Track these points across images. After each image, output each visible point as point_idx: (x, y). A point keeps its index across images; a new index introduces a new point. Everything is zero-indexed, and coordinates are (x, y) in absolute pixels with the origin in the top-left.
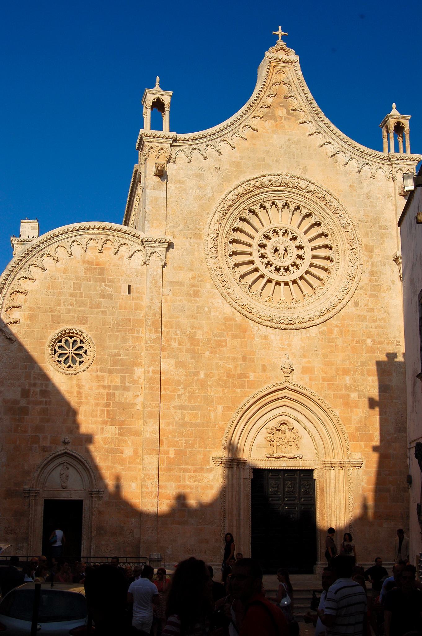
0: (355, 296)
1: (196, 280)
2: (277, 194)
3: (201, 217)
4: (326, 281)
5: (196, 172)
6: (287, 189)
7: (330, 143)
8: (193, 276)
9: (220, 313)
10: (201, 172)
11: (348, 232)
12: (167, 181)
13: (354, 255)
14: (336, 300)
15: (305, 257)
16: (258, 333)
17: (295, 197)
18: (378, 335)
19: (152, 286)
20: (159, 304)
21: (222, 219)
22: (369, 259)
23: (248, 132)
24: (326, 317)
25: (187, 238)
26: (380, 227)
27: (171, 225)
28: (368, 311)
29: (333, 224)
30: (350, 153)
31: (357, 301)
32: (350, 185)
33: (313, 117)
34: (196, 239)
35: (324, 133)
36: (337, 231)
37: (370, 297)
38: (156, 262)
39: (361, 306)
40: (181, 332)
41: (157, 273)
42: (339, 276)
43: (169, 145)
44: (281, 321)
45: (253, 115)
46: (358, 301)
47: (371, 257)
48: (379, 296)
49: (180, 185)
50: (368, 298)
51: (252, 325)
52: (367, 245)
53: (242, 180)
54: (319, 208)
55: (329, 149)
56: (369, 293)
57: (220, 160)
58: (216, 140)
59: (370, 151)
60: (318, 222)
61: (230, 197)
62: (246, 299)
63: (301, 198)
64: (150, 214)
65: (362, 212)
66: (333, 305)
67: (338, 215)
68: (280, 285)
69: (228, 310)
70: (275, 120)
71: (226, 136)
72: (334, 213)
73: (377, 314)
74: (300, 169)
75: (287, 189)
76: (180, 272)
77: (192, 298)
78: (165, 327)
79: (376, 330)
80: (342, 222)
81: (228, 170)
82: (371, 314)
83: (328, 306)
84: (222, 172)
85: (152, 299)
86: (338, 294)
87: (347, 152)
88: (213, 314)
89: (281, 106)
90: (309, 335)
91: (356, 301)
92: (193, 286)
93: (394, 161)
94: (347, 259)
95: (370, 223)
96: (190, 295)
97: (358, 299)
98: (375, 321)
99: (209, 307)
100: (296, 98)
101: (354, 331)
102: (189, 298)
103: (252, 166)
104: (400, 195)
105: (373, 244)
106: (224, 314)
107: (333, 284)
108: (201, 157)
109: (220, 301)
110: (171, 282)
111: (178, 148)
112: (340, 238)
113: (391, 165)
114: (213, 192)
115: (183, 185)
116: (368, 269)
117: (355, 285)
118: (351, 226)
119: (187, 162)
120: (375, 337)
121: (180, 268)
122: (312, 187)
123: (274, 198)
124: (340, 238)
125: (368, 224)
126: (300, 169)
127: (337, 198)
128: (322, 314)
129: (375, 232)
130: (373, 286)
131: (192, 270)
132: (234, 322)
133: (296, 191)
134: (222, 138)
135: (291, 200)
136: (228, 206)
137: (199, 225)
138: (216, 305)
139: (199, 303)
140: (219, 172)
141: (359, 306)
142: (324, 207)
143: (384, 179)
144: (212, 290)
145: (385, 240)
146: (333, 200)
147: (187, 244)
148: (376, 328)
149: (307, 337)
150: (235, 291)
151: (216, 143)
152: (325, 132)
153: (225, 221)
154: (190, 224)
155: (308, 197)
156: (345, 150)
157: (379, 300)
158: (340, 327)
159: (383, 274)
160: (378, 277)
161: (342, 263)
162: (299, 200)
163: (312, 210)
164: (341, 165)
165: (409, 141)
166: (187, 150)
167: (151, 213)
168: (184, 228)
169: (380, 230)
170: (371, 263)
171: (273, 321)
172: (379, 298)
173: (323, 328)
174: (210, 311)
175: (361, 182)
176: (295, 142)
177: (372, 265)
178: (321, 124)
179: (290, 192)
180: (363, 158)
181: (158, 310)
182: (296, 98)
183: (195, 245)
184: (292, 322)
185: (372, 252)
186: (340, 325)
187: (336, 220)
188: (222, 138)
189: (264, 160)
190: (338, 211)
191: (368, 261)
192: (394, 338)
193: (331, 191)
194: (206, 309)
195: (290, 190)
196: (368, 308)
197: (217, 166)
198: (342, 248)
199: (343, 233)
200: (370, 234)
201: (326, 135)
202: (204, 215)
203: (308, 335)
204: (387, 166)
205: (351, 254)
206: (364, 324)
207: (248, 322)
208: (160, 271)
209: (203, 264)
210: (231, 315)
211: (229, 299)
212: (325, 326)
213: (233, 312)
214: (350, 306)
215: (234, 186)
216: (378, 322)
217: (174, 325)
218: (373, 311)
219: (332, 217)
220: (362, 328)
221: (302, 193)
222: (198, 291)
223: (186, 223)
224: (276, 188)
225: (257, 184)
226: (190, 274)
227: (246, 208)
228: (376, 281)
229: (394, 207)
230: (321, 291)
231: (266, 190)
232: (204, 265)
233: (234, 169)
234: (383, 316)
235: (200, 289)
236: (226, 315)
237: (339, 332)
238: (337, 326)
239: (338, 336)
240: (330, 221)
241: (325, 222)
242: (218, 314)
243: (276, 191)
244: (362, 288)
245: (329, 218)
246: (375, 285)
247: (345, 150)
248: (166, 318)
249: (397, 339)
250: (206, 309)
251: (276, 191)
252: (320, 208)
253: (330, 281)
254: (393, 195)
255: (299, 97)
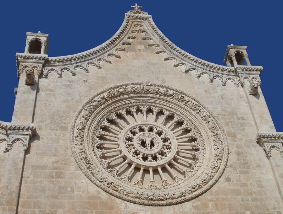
0: (225, 173)
1: (60, 163)
2: (141, 100)
3: (68, 115)
4: (194, 166)
5: (66, 84)
6: (149, 95)
7: (183, 64)
8: (57, 160)
9: (84, 192)
10: (69, 83)
11: (209, 122)
12: (38, 91)
13: (218, 139)
14: (207, 176)
15: (172, 147)
16: (125, 210)
17: (157, 102)
18: (257, 207)
19: (11, 168)
20: (18, 184)
21: (88, 115)
22: (234, 143)
23: (112, 59)
24: (199, 192)
25: (53, 130)
26: (238, 119)
27: (37, 120)
28: (241, 186)
29: (194, 119)
30: (201, 69)
31: (228, 177)
32: (205, 90)
33: (166, 48)
34: (62, 130)
35: (177, 58)
36: (199, 124)
37: (241, 174)
38: (19, 148)
39: (233, 182)
40: (39, 211)
41: (19, 157)
42: (206, 159)
43: (41, 64)
44: (151, 197)
45: (116, 47)
46: (229, 177)
47: (235, 141)
48: (250, 172)
49: (50, 92)
50: (238, 175)
51: (119, 203)
52: (229, 132)
53: (106, 87)
54: (180, 108)
55: (183, 68)
56: (239, 169)
57: (88, 76)
58: (84, 62)
59: (218, 66)
60: (181, 120)
61: (96, 99)
62: (111, 178)
63: (163, 102)
64: (18, 111)
65: (219, 109)
66: (204, 181)
67: (198, 111)
68: (149, 174)
69: (93, 189)
70: (135, 51)
71: (93, 60)
72: (193, 110)
73: (251, 187)
74: (159, 81)
75: (149, 95)
76: (43, 157)
77: (54, 179)
78: (22, 207)
79: (253, 202)
80: (202, 115)
81: (94, 82)
82: (245, 188)
83: (199, 181)
84: (89, 83)
85: (10, 179)
86: (208, 172)
87: (199, 68)
88: (76, 193)
89: (140, 44)
90: (183, 210)
91: (227, 177)
92: (56, 168)
93: (239, 71)
94: (212, 144)
95: (228, 116)
96: (53, 177)
97: (229, 175)
98: (250, 194)
99: (72, 188)
100: (152, 39)
101: (231, 204)
102: (51, 179)
103: (117, 79)
104: (251, 95)
105: (234, 131)
106: (89, 193)
107: (202, 166)
108: (71, 74)
109: (84, 181)
110: (33, 166)
111: (50, 68)
112: (202, 129)
113: (238, 76)
114: (81, 96)
115: (52, 93)
116: (234, 149)
117: (223, 163)
118: (211, 118)
119: (57, 77)
120: (254, 209)
121: (44, 154)
122: (171, 92)
123: (138, 104)
124: (202, 129)
125: (226, 117)
126: (159, 81)
127: (194, 98)
128: (193, 190)
129: (234, 122)
130: (242, 164)
131: (56, 156)
132: (99, 200)
133: (157, 96)
134: (89, 61)
135: (154, 104)
136: (94, 106)
137: (66, 120)
138: (79, 185)
139: (61, 184)
140: (87, 83)
141: (231, 181)
142: (185, 107)
143: (234, 86)
144: (76, 172)
145: (245, 128)
146: (190, 99)
147: (53, 134)
148: (253, 201)
149: (180, 212)
150: (100, 172)
151: (84, 64)
152: (178, 57)
153: (91, 118)
154: (57, 119)
155: (168, 100)
156: (197, 68)
157: (251, 176)
158: (215, 201)
159: (249, 154)
160: (245, 156)
161: (207, 148)
162: (161, 104)
163: (174, 111)
164: (195, 78)
165: (249, 61)
166: (59, 69)
167: (19, 110)
168: (51, 122)
169: (239, 121)
170: (235, 145)
171: (142, 197)
172: (250, 174)
173: (196, 202)
174: (73, 191)
175: (214, 88)
176: (153, 65)
177: (238, 147)
178: (174, 52)
179: (152, 98)
180: (213, 72)
181: (15, 190)
182: (152, 39)
183: (60, 136)
184: (162, 198)
185: (235, 137)
186: (215, 199)
187: (197, 116)
188: (89, 61)
189: (127, 75)
190: (197, 108)
191: (232, 144)
192: (275, 209)
193: (188, 93)
194: (69, 189)
195: (152, 96)
196: (241, 183)
197: (85, 79)
198: (206, 137)
199: (205, 124)
200: (230, 124)
201: (179, 59)
202: (71, 113)
203: (181, 210)
204: (234, 77)
205: (215, 139)
206: (240, 197)
207: (114, 200)
208: (22, 155)
209: (68, 150)
210: (96, 194)
211: (93, 178)
212: (199, 201)
213: (98, 191)
214: (222, 182)
215: (99, 91)
216: (254, 195)
217: (32, 204)
218: (247, 186)
219: (193, 114)
220: (239, 201)
221: (163, 97)
222: (61, 173)
223: (54, 119)
224: (139, 95)
225: (121, 90)
226: (53, 159)
227: (112, 111)
228: (244, 160)
229: (247, 104)
230: (191, 174)
231: (129, 96)
232: (69, 152)
233: (100, 81)
234: (258, 190)
235: (63, 171)
236: (90, 194)
237: (214, 206)
238: (211, 200)
239: (214, 210)
240: (191, 118)
241: (187, 119)
242: (81, 194)
243: (139, 97)
244: (231, 166)
245: (190, 115)
246: (244, 163)
247: (197, 68)
248: (24, 198)
249: (278, 210)
250: (69, 189)
251: (139, 97)
252: (181, 109)
253: (198, 165)
254: (245, 96)
255: (154, 38)
